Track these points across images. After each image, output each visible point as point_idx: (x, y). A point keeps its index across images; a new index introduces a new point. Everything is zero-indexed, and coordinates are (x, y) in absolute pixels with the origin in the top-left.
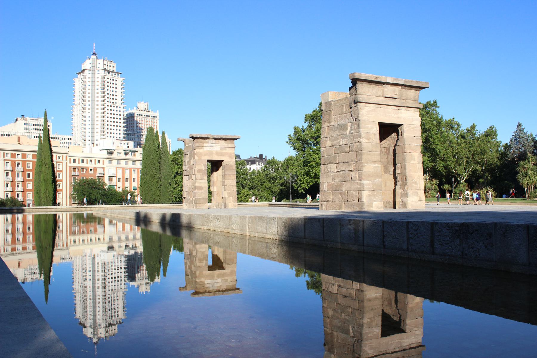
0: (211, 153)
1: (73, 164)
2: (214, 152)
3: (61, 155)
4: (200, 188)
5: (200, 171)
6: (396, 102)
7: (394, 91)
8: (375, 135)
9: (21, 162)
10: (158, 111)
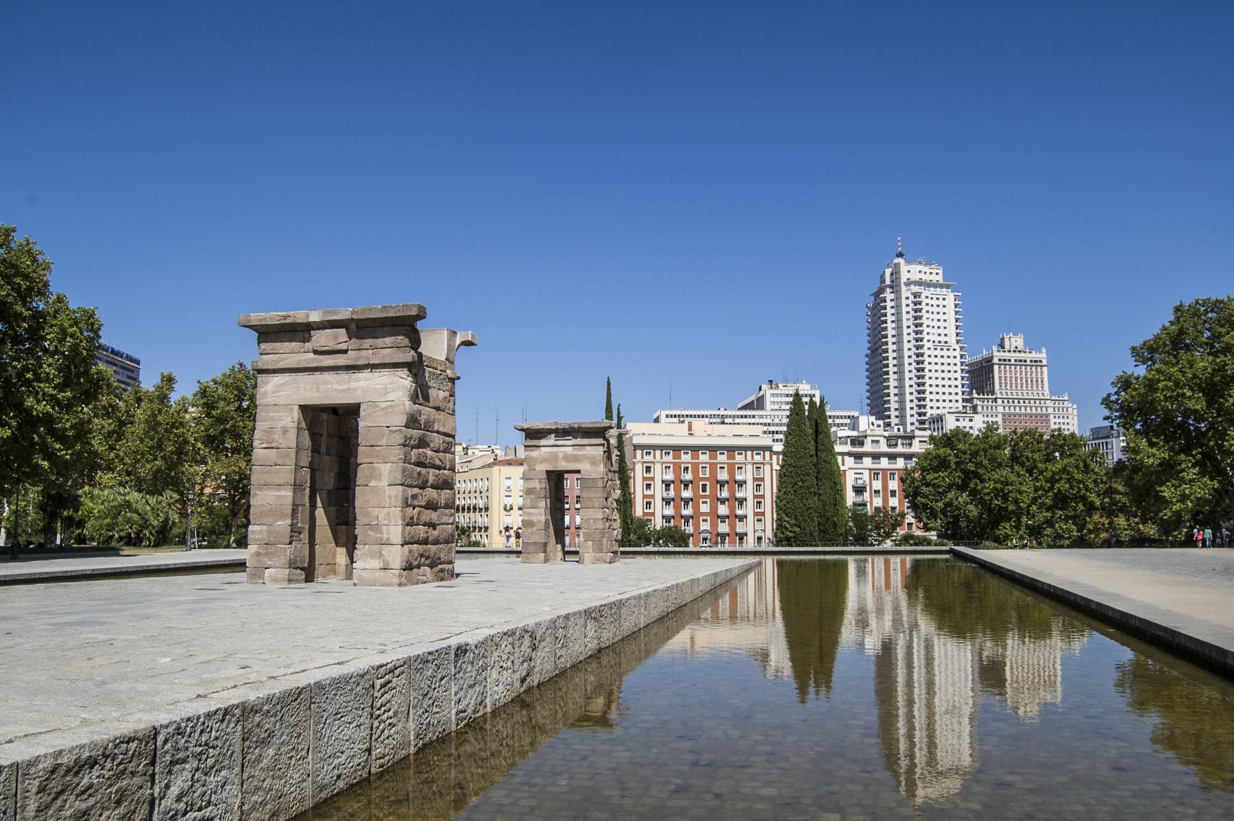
0: (554, 457)
2: (561, 455)
6: (340, 360)
7: (336, 337)
10: (1044, 350)
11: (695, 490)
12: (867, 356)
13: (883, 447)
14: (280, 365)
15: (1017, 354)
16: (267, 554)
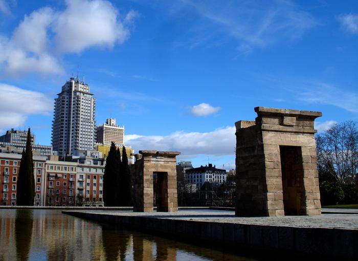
0: (156, 166)
1: (49, 171)
2: (159, 165)
3: (41, 163)
4: (148, 195)
5: (147, 180)
6: (294, 129)
8: (276, 155)
9: (8, 168)
11: (10, 180)
12: (53, 122)
13: (92, 165)
14: (272, 129)
15: (113, 127)
16: (276, 204)
